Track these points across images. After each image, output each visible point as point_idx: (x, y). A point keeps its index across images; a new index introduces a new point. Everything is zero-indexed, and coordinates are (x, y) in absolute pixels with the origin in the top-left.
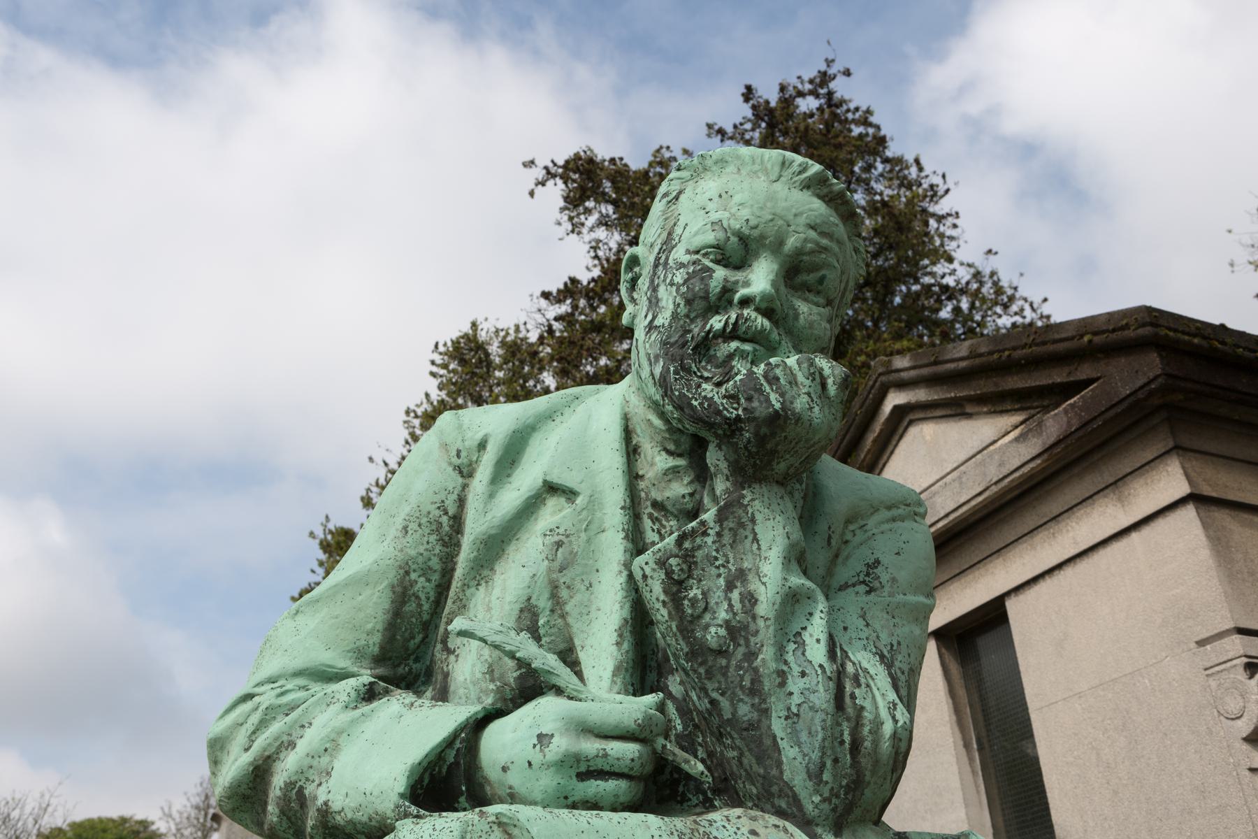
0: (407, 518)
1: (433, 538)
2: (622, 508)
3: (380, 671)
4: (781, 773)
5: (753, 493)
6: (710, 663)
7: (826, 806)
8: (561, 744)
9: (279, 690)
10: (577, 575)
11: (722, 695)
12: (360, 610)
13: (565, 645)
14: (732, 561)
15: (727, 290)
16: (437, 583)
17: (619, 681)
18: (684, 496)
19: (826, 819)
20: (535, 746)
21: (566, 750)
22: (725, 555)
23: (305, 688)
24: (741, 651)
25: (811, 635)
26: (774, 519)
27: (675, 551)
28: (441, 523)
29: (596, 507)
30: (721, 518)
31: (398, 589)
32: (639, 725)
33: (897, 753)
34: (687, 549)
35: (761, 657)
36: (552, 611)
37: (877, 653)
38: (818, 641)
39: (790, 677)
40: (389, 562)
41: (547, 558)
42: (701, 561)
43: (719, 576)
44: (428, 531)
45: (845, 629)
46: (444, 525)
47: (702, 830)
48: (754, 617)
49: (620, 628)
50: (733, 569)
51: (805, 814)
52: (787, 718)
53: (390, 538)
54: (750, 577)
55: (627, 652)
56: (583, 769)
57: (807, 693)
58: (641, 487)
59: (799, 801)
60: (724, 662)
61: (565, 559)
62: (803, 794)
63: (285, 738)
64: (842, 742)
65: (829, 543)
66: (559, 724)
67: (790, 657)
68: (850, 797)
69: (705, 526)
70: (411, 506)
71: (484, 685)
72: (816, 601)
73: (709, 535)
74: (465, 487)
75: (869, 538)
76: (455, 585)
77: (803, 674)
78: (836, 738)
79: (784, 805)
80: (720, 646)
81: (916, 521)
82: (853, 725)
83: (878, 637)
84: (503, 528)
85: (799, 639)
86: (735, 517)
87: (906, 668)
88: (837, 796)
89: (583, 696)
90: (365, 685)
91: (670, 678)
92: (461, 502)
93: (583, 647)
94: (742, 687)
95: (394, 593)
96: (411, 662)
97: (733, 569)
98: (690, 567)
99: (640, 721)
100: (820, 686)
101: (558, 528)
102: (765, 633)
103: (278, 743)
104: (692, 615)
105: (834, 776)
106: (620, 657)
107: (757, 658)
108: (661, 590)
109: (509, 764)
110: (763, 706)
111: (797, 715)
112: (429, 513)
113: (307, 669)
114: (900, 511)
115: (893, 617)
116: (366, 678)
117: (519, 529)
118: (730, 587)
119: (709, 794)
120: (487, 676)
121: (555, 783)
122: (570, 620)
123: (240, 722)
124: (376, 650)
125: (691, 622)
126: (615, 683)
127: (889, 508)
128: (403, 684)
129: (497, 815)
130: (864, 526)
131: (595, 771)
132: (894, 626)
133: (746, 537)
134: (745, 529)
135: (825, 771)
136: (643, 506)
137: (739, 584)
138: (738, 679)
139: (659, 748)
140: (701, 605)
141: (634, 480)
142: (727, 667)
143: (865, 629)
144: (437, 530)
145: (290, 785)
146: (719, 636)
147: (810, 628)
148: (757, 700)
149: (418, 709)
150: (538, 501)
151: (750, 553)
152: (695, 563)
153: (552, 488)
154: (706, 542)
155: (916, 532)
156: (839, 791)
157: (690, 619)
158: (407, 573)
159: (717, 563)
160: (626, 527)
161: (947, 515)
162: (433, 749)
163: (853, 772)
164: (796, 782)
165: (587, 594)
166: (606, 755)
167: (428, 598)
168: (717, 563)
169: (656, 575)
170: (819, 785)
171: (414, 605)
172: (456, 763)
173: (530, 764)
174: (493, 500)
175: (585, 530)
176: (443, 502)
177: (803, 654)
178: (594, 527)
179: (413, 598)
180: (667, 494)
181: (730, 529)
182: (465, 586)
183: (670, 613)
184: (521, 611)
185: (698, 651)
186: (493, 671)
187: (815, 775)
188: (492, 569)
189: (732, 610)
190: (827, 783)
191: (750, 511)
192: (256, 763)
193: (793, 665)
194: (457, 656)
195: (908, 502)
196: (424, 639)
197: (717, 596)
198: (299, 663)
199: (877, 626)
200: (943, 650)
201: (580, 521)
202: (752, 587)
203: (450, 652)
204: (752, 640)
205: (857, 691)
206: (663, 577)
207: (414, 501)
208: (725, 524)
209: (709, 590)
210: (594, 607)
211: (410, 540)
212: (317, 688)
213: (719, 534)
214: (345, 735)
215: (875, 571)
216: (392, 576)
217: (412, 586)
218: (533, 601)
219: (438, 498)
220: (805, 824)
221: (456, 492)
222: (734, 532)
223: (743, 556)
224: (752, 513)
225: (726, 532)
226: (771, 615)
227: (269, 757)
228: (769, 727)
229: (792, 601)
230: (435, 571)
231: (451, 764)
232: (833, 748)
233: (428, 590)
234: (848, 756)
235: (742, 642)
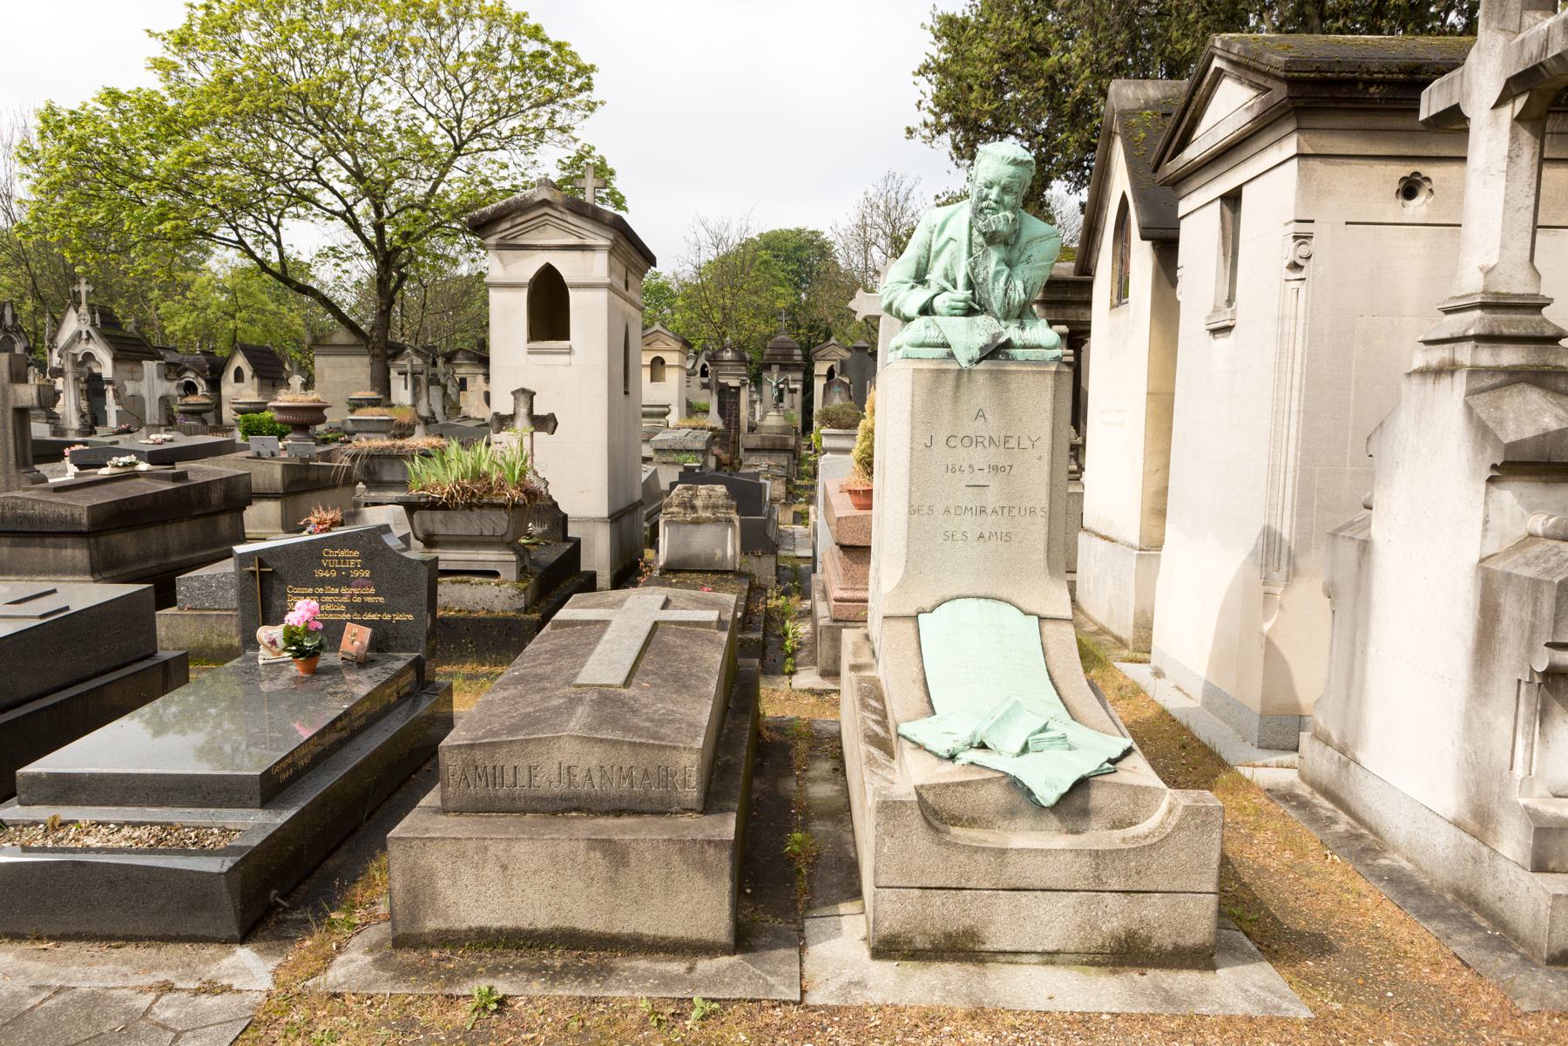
8: (948, 303)
15: (987, 196)
102: (990, 281)
220: (998, 319)
229: (998, 273)
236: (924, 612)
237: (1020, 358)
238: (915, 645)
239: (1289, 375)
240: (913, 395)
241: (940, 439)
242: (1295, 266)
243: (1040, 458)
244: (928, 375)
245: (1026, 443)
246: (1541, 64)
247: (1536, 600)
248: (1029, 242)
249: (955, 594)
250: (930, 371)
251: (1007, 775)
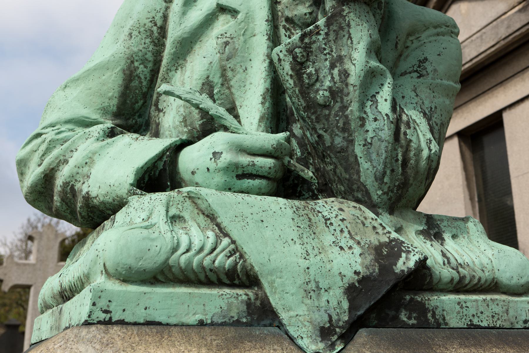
0: (131, 28)
1: (148, 41)
2: (267, 21)
3: (118, 122)
4: (359, 177)
5: (349, 8)
6: (319, 113)
7: (385, 197)
8: (227, 158)
9: (57, 131)
10: (238, 63)
11: (325, 132)
12: (104, 84)
13: (230, 105)
14: (334, 51)
16: (151, 69)
17: (263, 125)
18: (305, 14)
19: (385, 204)
20: (211, 159)
21: (230, 161)
22: (330, 47)
23: (72, 130)
24: (338, 105)
25: (382, 97)
26: (362, 25)
27: (299, 44)
28: (153, 31)
29: (250, 21)
30: (328, 24)
31: (127, 72)
32: (274, 148)
33: (430, 169)
34: (306, 43)
35: (350, 109)
36: (222, 85)
37: (422, 112)
38: (386, 100)
39: (367, 121)
40: (121, 55)
41: (219, 52)
42: (315, 51)
43: (326, 60)
44: (144, 36)
45: (403, 97)
46: (155, 32)
47: (310, 207)
48: (347, 85)
49: (264, 94)
50: (335, 55)
51: (372, 201)
52: (364, 145)
53: (122, 40)
54: (345, 60)
55: (268, 108)
56: (240, 172)
57: (377, 130)
58: (279, 9)
59: (369, 193)
60: (327, 112)
61: (230, 53)
62: (371, 190)
63: (62, 158)
64: (397, 160)
65: (396, 47)
66: (226, 146)
67: (368, 110)
68: (400, 192)
69: (318, 29)
70: (133, 21)
71: (180, 129)
72: (386, 77)
73: (320, 34)
74: (167, 8)
75: (422, 45)
76: (163, 69)
77: (376, 120)
78: (393, 158)
79: (360, 196)
80: (325, 102)
81: (452, 37)
82: (404, 150)
83: (423, 103)
84: (191, 34)
85: (374, 99)
86: (337, 23)
87: (439, 122)
88: (392, 191)
89: (241, 132)
90: (108, 128)
91: (294, 125)
92: (165, 18)
93: (241, 106)
94: (338, 127)
95: (125, 74)
96: (136, 117)
97: (335, 55)
98: (308, 54)
99: (275, 146)
100: (386, 126)
101: (226, 33)
103: (58, 161)
104: (308, 84)
105: (391, 180)
106: (263, 111)
107: (347, 110)
108: (289, 68)
109: (196, 170)
110: (350, 138)
111: (371, 144)
112: (145, 25)
113: (73, 119)
114: (442, 30)
115: (433, 92)
116: (109, 124)
117: (201, 35)
118: (333, 66)
119: (316, 192)
120: (183, 124)
121: (223, 180)
122: (233, 90)
123: (35, 149)
124: (115, 109)
125: (308, 88)
126: (260, 126)
127: (435, 27)
128: (132, 130)
129: (188, 193)
130: (419, 37)
131: (247, 174)
132: (434, 97)
133: (344, 36)
134: (343, 31)
135: (386, 176)
136: (280, 21)
137: (338, 65)
138: (336, 122)
139: (286, 162)
140: (315, 77)
141: (274, 5)
142: (329, 115)
143: (415, 98)
144: (150, 36)
145: (66, 184)
146: (324, 96)
147: (381, 93)
148: (346, 135)
149: (141, 141)
150: (214, 17)
151: (346, 46)
152: (312, 52)
153: (222, 9)
154: (318, 39)
155: (452, 43)
156: (393, 189)
157: (307, 86)
158: (132, 62)
159: (325, 52)
160: (269, 33)
161: (471, 60)
162: (150, 160)
163: (403, 178)
164: (368, 183)
165: (244, 75)
166: (254, 165)
167: (146, 78)
168: (325, 52)
169: (286, 59)
170: (381, 185)
171: (137, 82)
172: (164, 169)
173: (208, 169)
174: (185, 16)
175: (243, 35)
176: (153, 18)
177: (376, 108)
178: (248, 33)
179: (136, 78)
180: (295, 13)
181: (334, 31)
182: (169, 70)
183: (294, 83)
184: (203, 84)
186: (186, 120)
187: (380, 179)
188: (185, 60)
189: (333, 81)
190: (386, 183)
191: (347, 19)
192: (46, 172)
193: (369, 114)
194: (164, 113)
195: (448, 24)
196: (144, 103)
197: (324, 72)
198: (68, 115)
199: (423, 96)
200: (462, 144)
201: (240, 29)
202: (346, 67)
203: (160, 111)
204: (345, 98)
205: (408, 131)
206: (291, 60)
207: (135, 17)
208: (331, 27)
209: (319, 69)
210: (248, 83)
211: (133, 42)
212: (80, 131)
213: (327, 34)
214: (97, 154)
215: (424, 64)
216: (123, 64)
217: (135, 70)
218: (210, 78)
219: (150, 15)
221: (162, 12)
222: (336, 32)
223: (341, 48)
224: (349, 21)
225: (331, 32)
226: (358, 83)
227: (53, 169)
228: (353, 150)
230: (150, 61)
231: (161, 170)
232: (391, 163)
233: (146, 73)
234: (400, 168)
235: (339, 100)
237: (454, 322)
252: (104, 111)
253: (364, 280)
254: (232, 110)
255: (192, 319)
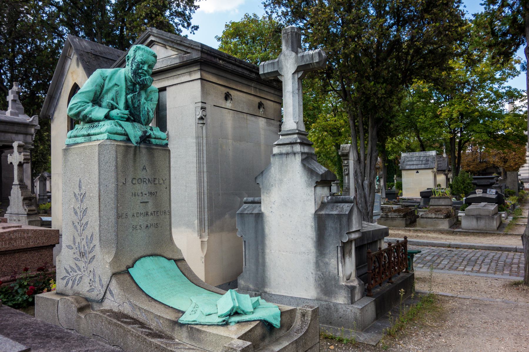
92: (104, 84)
153: (116, 84)
185: (134, 107)
207: (97, 82)
216: (94, 92)
236: (130, 268)
238: (134, 285)
239: (202, 158)
240: (117, 158)
241: (129, 180)
242: (201, 118)
243: (166, 188)
244: (123, 148)
245: (161, 182)
246: (311, 64)
247: (340, 221)
248: (150, 92)
249: (140, 255)
250: (123, 146)
251: (261, 321)
252: (90, 100)
253: (142, 136)
254: (117, 104)
255: (120, 140)
